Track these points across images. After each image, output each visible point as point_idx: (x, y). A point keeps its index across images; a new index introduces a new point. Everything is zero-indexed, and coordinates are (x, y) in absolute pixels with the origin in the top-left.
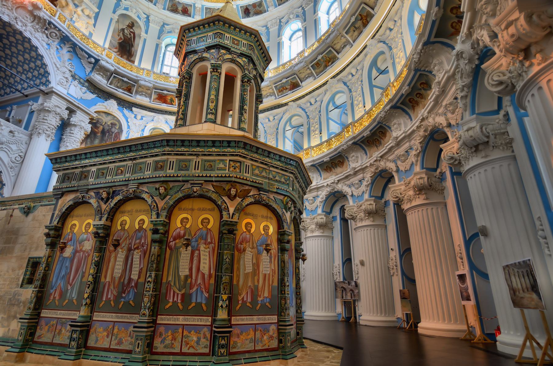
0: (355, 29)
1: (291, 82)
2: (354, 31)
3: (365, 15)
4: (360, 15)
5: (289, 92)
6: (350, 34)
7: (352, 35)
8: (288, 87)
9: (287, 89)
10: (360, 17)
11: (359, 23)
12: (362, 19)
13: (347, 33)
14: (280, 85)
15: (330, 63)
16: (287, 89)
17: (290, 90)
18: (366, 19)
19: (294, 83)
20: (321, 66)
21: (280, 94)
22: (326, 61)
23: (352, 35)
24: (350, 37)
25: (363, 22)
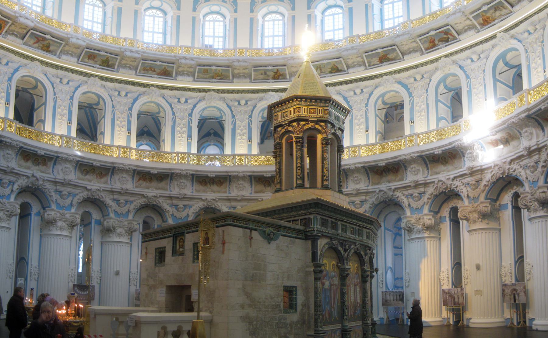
0: (263, 73)
1: (165, 68)
2: (262, 74)
3: (281, 73)
4: (278, 70)
5: (156, 76)
6: (256, 73)
7: (257, 75)
8: (158, 71)
9: (154, 71)
10: (276, 71)
11: (272, 74)
12: (276, 73)
13: (255, 71)
14: (150, 65)
15: (219, 78)
16: (154, 71)
17: (158, 74)
18: (279, 76)
19: (167, 71)
20: (207, 74)
21: (142, 72)
22: (216, 74)
23: (257, 75)
24: (254, 75)
25: (275, 75)
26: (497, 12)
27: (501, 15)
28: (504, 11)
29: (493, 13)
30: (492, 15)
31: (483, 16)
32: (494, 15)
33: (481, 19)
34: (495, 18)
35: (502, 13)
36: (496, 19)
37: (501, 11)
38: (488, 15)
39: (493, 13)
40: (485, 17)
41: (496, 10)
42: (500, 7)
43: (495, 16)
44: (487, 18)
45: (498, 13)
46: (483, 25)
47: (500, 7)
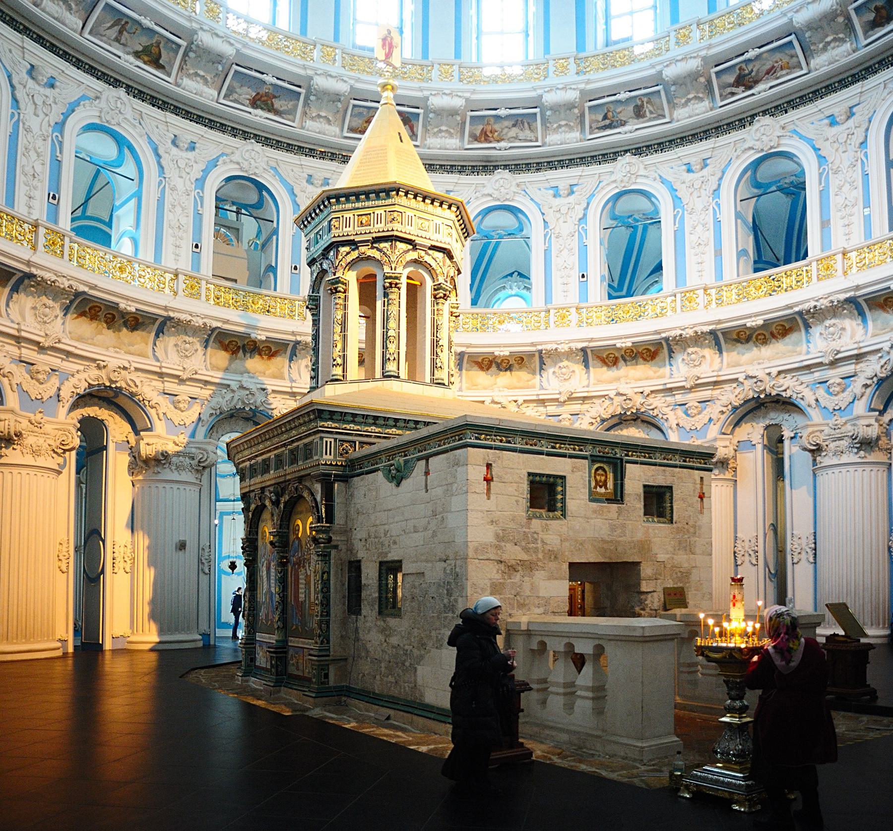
26: (514, 128)
27: (516, 138)
28: (527, 133)
29: (507, 127)
30: (502, 129)
31: (488, 124)
32: (506, 130)
33: (481, 127)
34: (504, 137)
35: (521, 135)
36: (503, 140)
37: (522, 130)
38: (497, 127)
39: (507, 127)
40: (489, 128)
41: (514, 125)
42: (526, 124)
43: (506, 134)
44: (491, 132)
45: (514, 132)
46: (476, 140)
47: (526, 124)
